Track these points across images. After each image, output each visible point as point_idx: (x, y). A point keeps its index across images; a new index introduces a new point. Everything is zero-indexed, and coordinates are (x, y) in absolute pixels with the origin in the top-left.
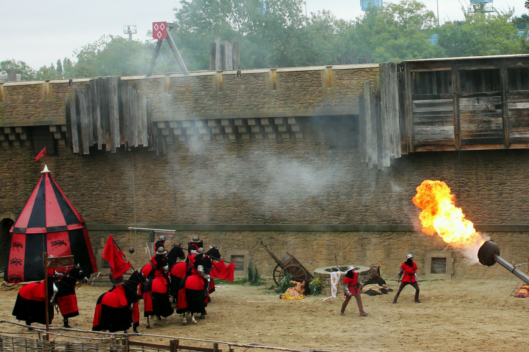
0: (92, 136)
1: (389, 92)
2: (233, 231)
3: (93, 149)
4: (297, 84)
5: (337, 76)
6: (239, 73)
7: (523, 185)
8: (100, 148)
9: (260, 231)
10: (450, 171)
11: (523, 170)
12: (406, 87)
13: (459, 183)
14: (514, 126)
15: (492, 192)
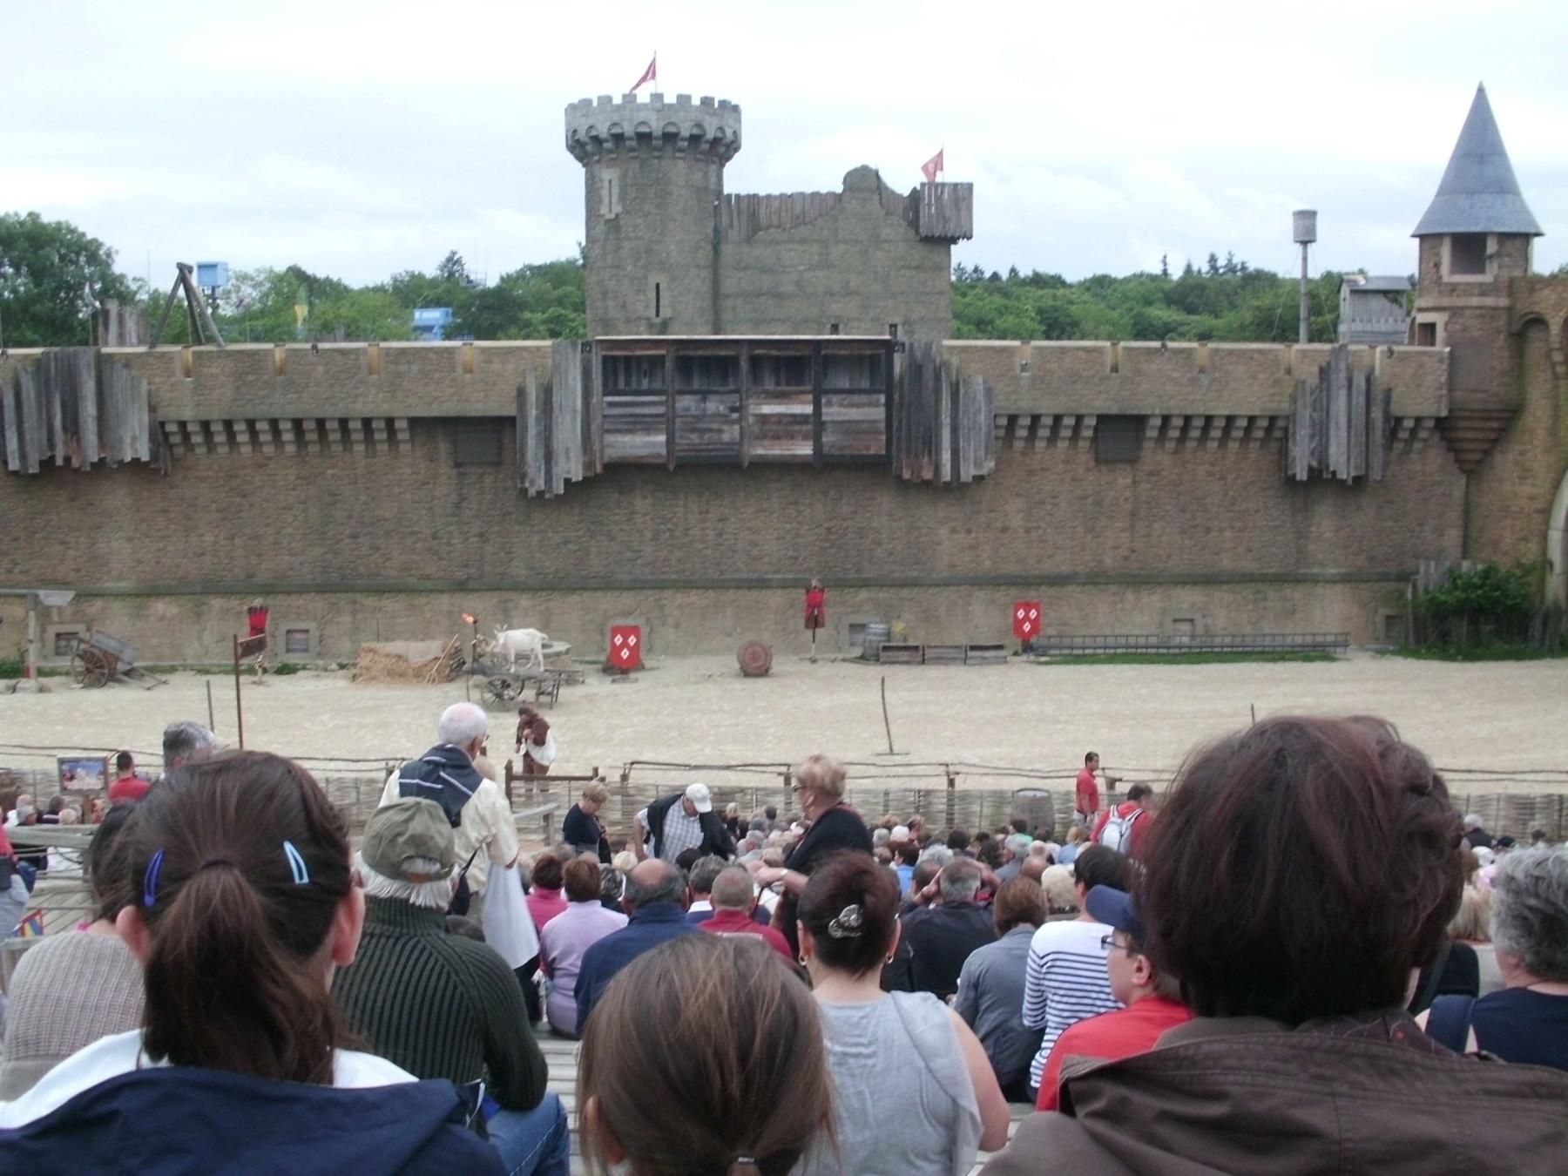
0: (45, 443)
1: (567, 383)
2: (289, 593)
3: (47, 464)
4: (415, 368)
6: (315, 347)
8: (59, 462)
9: (335, 592)
14: (757, 438)
15: (708, 531)
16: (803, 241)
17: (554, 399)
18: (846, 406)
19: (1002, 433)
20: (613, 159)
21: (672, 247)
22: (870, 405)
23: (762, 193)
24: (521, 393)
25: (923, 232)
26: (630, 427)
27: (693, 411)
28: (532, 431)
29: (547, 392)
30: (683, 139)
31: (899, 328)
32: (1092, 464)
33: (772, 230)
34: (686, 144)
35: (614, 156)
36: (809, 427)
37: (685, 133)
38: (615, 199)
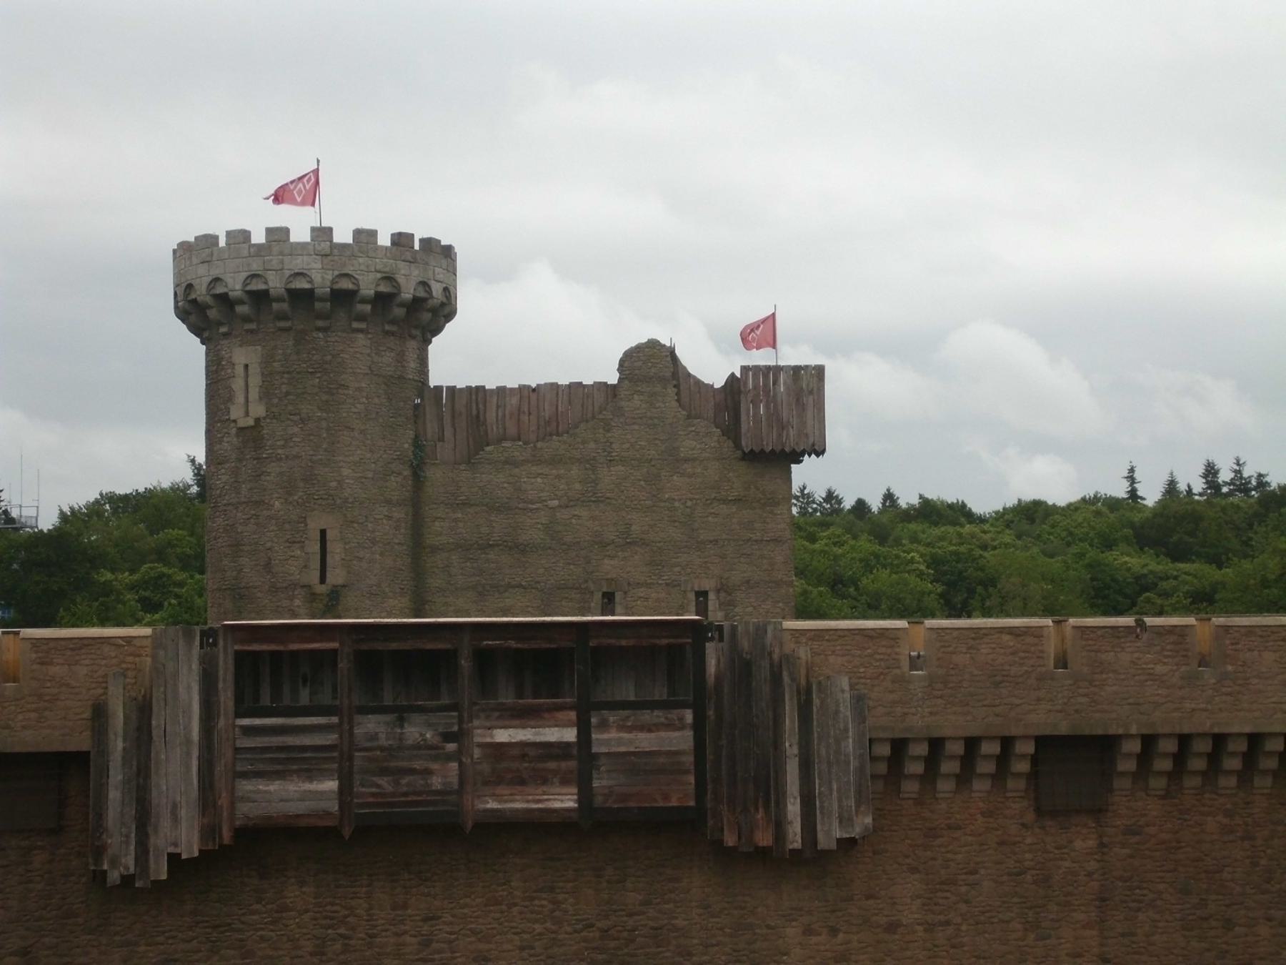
5: (34, 656)
7: (481, 920)
10: (304, 889)
11: (483, 887)
12: (221, 685)
13: (326, 918)
14: (486, 783)
15: (408, 939)
16: (555, 461)
17: (154, 723)
18: (630, 729)
19: (882, 768)
20: (252, 331)
21: (346, 472)
22: (669, 726)
23: (491, 385)
24: (99, 713)
25: (747, 444)
26: (279, 767)
27: (383, 741)
28: (116, 776)
29: (143, 711)
30: (364, 301)
31: (712, 596)
32: (1030, 816)
33: (507, 444)
34: (368, 308)
35: (253, 326)
36: (573, 764)
37: (368, 290)
38: (254, 394)
